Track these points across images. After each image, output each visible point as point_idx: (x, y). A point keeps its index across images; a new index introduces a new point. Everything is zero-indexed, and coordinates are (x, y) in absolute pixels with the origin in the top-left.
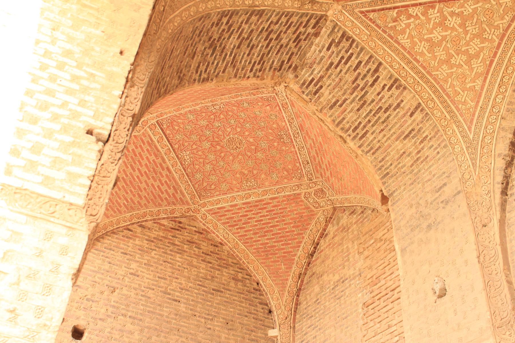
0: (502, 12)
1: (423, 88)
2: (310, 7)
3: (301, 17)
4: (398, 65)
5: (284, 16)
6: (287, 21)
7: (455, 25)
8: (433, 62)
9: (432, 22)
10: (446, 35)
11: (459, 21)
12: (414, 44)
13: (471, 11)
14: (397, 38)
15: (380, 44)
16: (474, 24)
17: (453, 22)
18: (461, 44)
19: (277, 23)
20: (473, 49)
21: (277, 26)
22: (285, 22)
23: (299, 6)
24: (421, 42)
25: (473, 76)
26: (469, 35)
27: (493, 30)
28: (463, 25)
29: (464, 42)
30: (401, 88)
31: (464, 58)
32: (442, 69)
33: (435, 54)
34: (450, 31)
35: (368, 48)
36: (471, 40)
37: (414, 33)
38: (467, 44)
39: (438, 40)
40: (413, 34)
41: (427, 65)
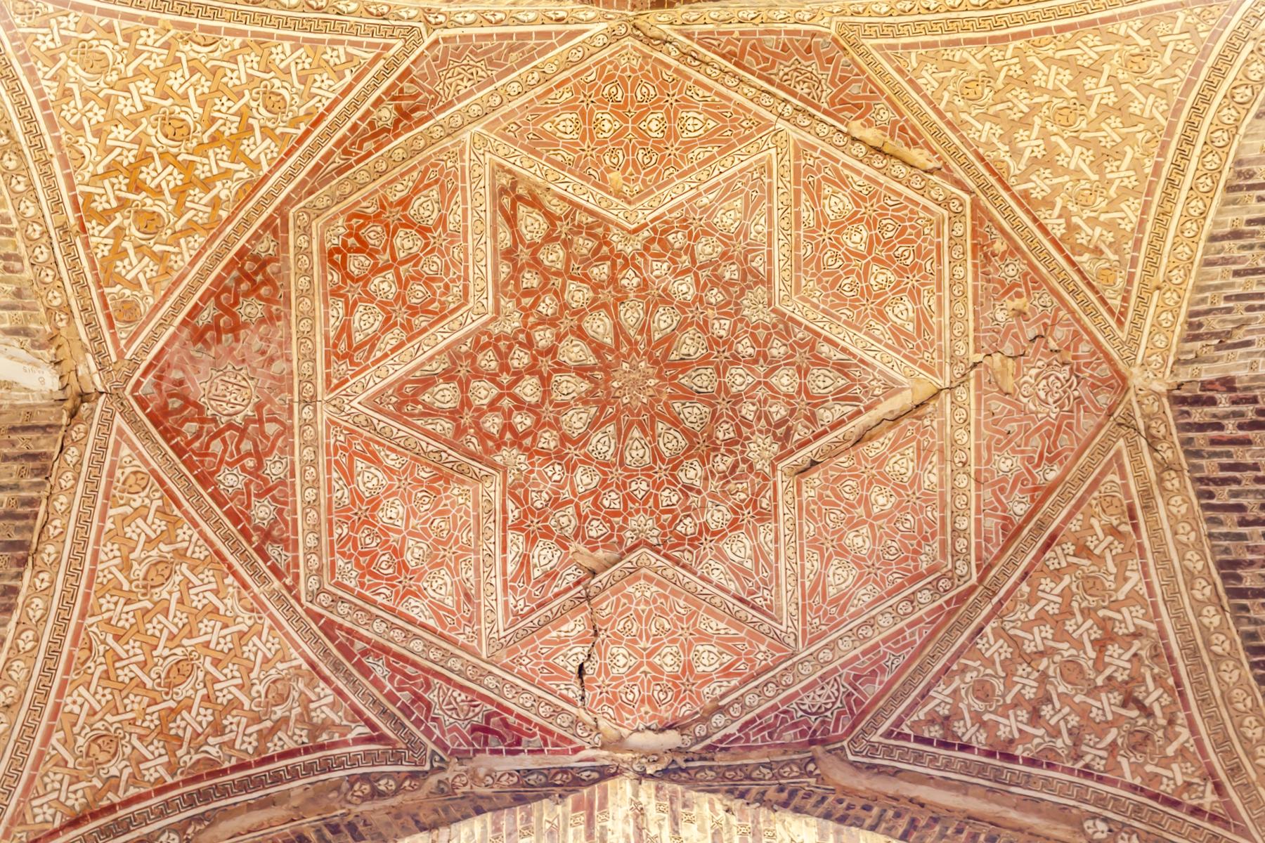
0: (954, 71)
1: (1213, 128)
2: (1165, 445)
3: (1198, 454)
4: (1193, 203)
5: (1214, 501)
6: (1225, 481)
7: (1034, 136)
8: (1140, 136)
9: (1055, 181)
10: (1065, 140)
11: (1021, 133)
12: (1124, 192)
13: (988, 125)
14: (1133, 230)
15: (1165, 260)
16: (1010, 104)
17: (1030, 143)
18: (1065, 104)
19: (1240, 508)
20: (1060, 77)
21: (1242, 501)
22: (1227, 488)
23: (1173, 474)
24: (1110, 182)
25: (1118, 46)
26: (1036, 100)
27: (997, 64)
28: (1025, 122)
29: (1055, 101)
30: (1244, 168)
31: (1089, 83)
32: (1143, 111)
33: (1119, 140)
34: (1053, 139)
35: (1191, 282)
36: (1043, 90)
37: (1101, 203)
38: (1056, 92)
39: (1084, 150)
40: (1104, 204)
41: (1153, 144)
